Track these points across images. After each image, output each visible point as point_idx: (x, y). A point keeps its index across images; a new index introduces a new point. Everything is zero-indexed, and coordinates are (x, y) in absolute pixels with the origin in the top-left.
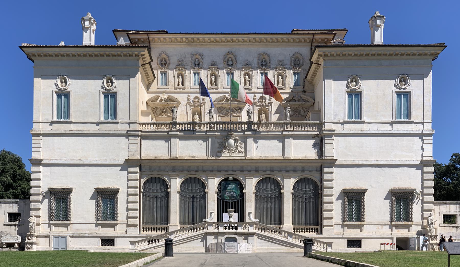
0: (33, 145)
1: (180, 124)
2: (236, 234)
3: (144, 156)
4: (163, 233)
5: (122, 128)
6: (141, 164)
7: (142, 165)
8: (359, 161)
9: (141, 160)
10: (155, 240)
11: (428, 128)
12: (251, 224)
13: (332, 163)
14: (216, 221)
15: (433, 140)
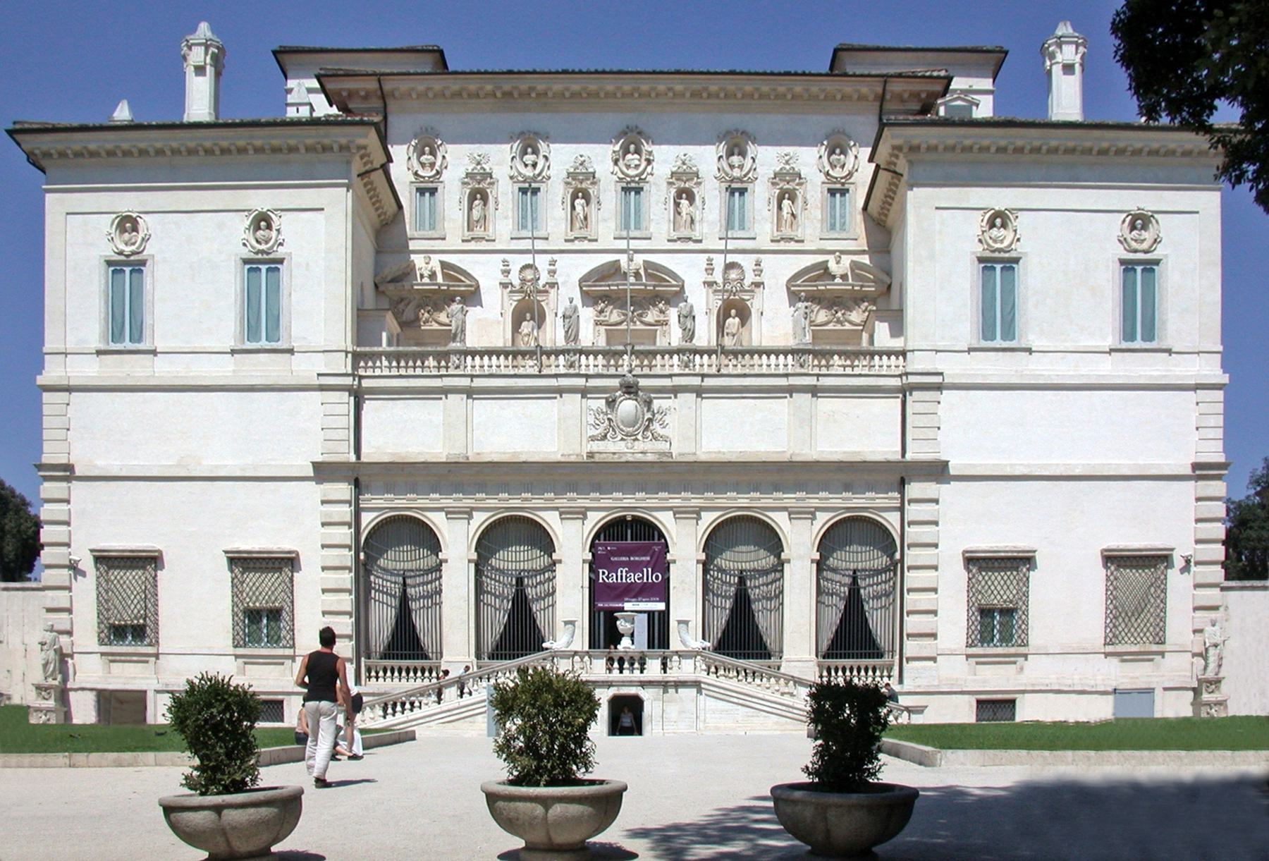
0: (47, 422)
1: (474, 353)
2: (643, 684)
3: (368, 454)
4: (419, 683)
5: (305, 368)
6: (359, 477)
7: (361, 479)
8: (1011, 465)
9: (359, 464)
10: (395, 705)
11: (1212, 370)
12: (692, 654)
13: (938, 471)
14: (586, 648)
15: (1226, 402)
